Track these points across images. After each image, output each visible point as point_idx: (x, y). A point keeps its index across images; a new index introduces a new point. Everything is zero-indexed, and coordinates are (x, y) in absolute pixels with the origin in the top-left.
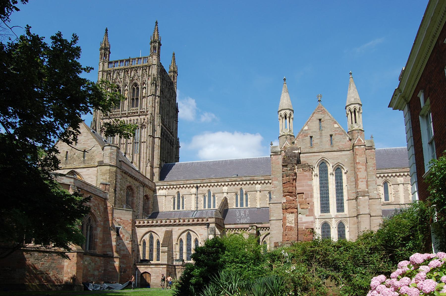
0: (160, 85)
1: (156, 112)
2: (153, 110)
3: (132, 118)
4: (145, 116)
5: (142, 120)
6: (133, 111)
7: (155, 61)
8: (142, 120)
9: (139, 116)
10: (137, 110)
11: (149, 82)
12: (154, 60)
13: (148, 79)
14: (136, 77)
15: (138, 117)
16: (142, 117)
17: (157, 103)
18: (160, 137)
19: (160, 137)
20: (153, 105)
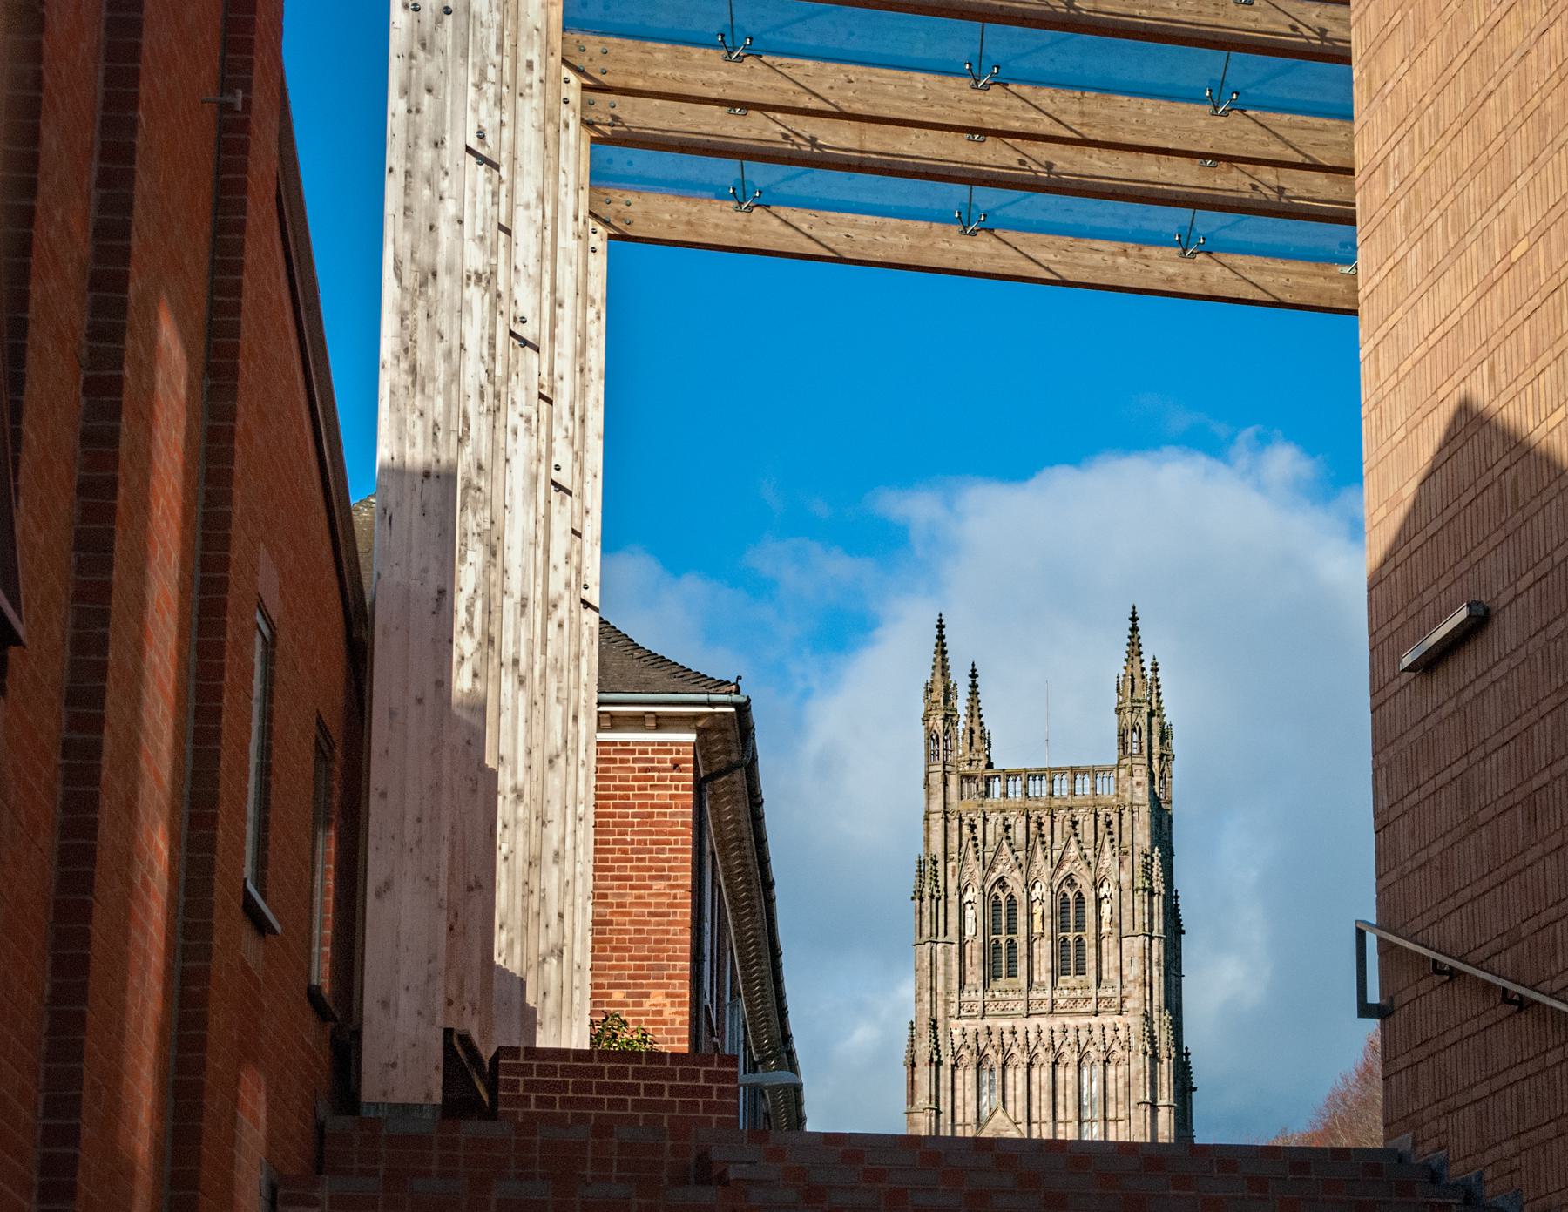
0: (1163, 892)
1: (1156, 1003)
2: (1148, 997)
3: (1071, 1022)
4: (1116, 1018)
5: (1109, 1033)
6: (1073, 995)
7: (1141, 788)
8: (1109, 1033)
9: (1097, 1014)
10: (1086, 992)
11: (1125, 877)
12: (1139, 784)
13: (1120, 863)
14: (1073, 851)
15: (1094, 1020)
16: (1108, 1020)
17: (1158, 964)
18: (1172, 1103)
19: (1172, 1103)
20: (1147, 978)
